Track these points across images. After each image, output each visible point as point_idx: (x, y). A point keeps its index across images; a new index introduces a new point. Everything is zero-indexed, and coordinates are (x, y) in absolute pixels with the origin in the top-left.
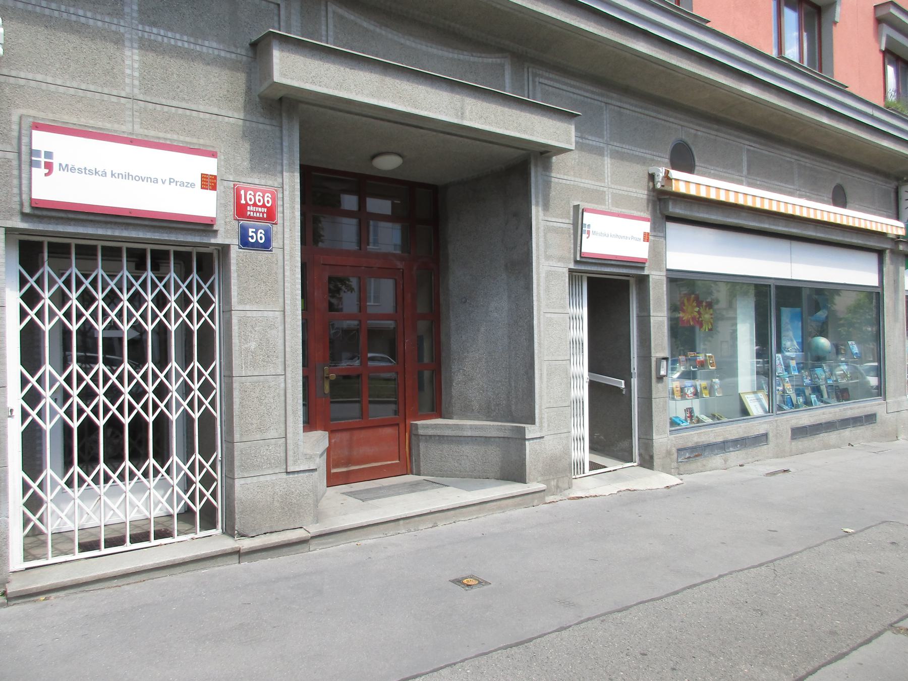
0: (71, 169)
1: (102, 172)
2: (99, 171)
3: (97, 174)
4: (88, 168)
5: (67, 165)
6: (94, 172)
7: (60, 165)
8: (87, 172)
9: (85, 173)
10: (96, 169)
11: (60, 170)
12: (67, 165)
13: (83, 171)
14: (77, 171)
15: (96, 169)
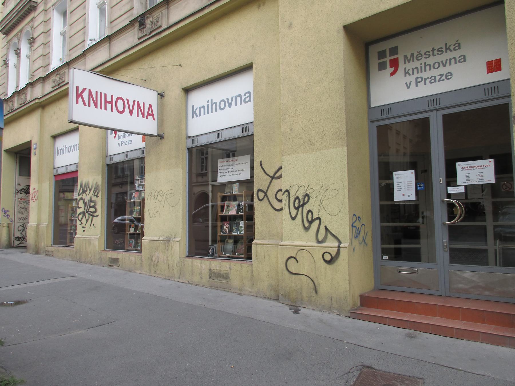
0: (417, 57)
1: (454, 45)
2: (450, 46)
3: (448, 51)
4: (436, 48)
5: (412, 55)
6: (444, 50)
7: (405, 57)
8: (436, 52)
9: (434, 55)
10: (446, 45)
11: (405, 63)
12: (412, 55)
13: (431, 53)
14: (424, 56)
15: (446, 45)
